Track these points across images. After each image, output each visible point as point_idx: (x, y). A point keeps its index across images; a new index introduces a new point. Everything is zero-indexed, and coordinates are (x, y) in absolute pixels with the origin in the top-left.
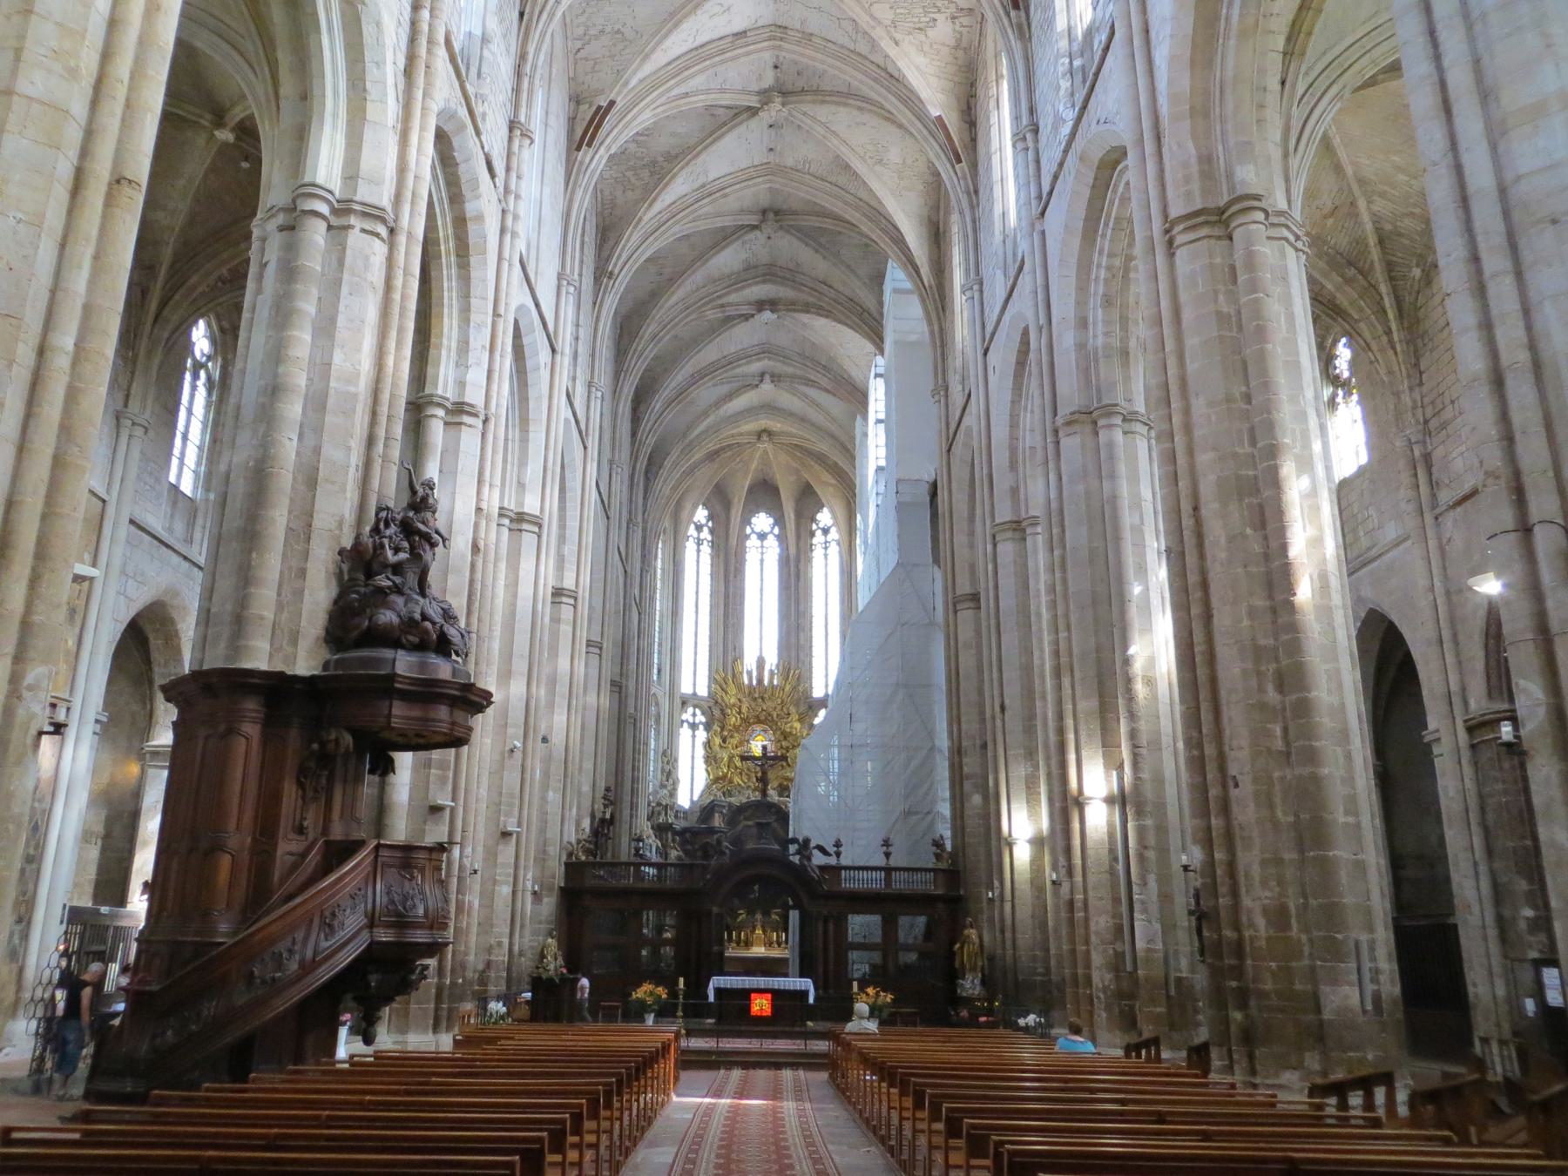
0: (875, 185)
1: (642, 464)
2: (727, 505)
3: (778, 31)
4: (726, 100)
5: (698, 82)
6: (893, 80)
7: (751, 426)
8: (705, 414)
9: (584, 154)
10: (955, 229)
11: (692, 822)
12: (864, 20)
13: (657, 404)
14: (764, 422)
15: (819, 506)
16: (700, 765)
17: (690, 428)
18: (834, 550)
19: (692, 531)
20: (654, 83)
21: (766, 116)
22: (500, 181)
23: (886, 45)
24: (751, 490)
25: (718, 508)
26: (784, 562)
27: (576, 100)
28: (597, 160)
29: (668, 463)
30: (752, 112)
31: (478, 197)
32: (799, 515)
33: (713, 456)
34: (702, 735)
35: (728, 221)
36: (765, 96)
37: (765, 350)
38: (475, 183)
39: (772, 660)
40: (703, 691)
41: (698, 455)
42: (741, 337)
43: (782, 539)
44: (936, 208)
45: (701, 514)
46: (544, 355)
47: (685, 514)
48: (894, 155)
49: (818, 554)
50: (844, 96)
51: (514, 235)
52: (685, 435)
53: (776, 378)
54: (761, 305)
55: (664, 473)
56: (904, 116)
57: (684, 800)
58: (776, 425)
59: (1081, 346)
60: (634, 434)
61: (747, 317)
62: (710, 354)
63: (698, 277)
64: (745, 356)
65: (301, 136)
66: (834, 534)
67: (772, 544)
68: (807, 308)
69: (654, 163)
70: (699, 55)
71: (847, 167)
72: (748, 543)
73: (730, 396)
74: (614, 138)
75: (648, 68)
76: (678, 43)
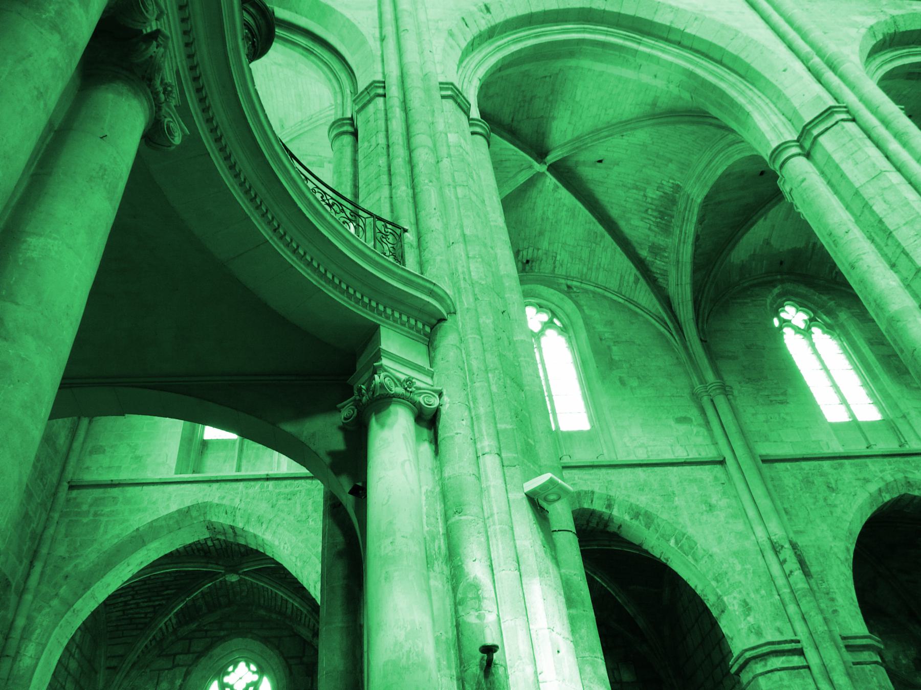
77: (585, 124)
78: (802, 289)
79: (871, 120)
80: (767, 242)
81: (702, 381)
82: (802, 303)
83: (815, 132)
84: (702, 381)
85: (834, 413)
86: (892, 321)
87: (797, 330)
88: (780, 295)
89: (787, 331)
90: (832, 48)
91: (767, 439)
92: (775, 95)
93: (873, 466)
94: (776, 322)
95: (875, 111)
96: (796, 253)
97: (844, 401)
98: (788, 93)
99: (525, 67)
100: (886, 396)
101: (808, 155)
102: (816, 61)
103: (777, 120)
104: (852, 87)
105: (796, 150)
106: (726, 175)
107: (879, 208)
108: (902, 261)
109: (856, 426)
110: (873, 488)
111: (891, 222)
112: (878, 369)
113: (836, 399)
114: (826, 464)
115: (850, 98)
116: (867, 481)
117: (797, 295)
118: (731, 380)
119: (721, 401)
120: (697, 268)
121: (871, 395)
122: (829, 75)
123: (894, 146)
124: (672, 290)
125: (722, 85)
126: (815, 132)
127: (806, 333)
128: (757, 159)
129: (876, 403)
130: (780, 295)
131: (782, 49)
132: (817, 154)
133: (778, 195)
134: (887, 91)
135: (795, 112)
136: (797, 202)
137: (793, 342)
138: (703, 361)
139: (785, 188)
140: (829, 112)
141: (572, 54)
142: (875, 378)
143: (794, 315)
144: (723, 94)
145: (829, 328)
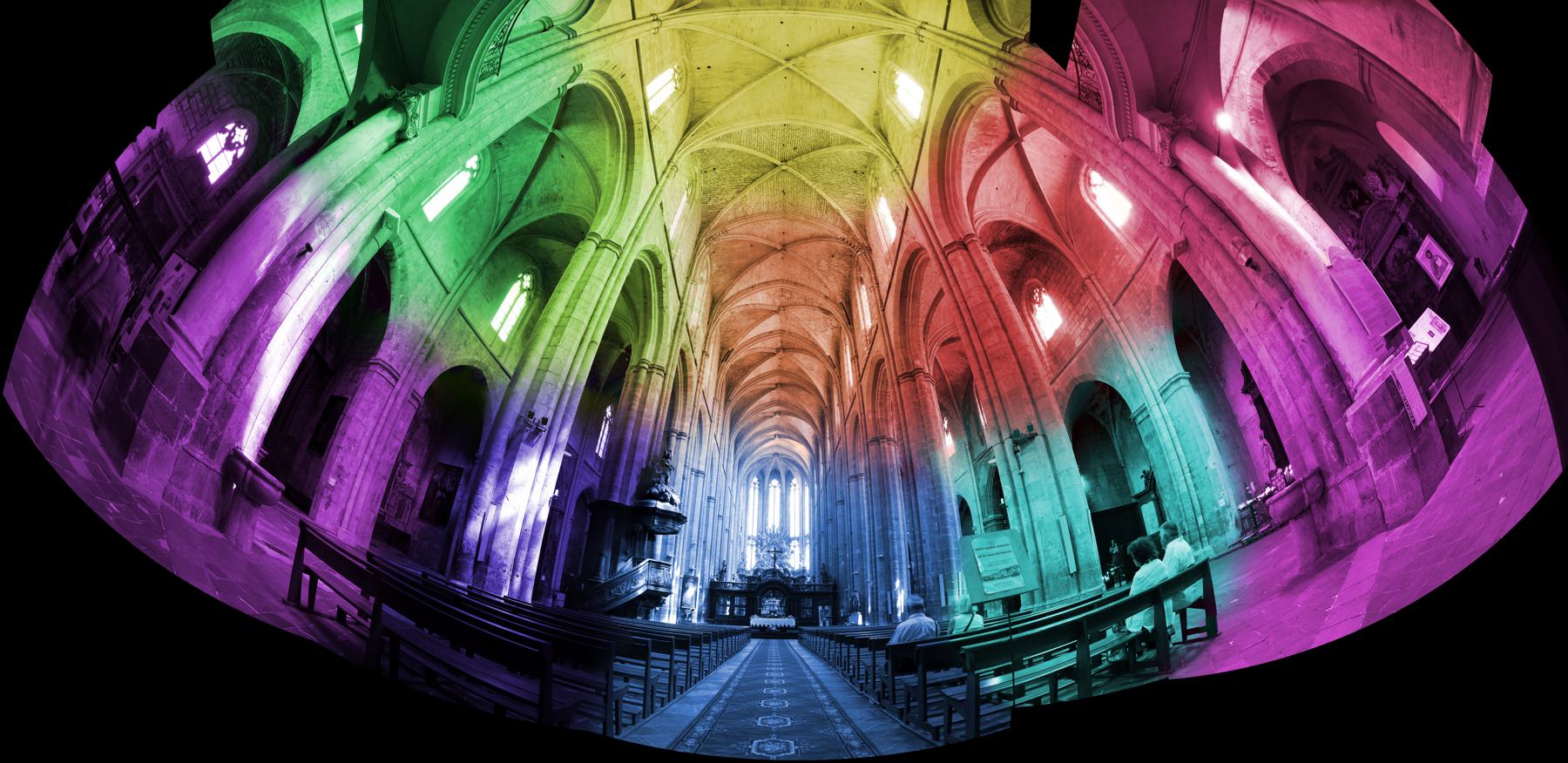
0: (810, 376)
1: (737, 462)
2: (764, 477)
3: (782, 332)
4: (767, 351)
5: (758, 345)
6: (816, 345)
8: (757, 447)
9: (724, 364)
10: (835, 389)
11: (751, 574)
12: (806, 328)
13: (743, 443)
14: (776, 450)
15: (793, 477)
16: (754, 558)
17: (753, 451)
20: (745, 345)
21: (778, 356)
23: (813, 335)
24: (772, 472)
26: (782, 495)
27: (722, 348)
28: (727, 366)
30: (774, 354)
33: (759, 461)
34: (755, 548)
35: (766, 387)
36: (778, 350)
37: (776, 428)
39: (777, 526)
40: (755, 535)
41: (755, 460)
42: (769, 423)
43: (781, 487)
44: (828, 383)
45: (755, 480)
48: (816, 368)
49: (792, 493)
50: (802, 350)
53: (780, 436)
54: (775, 413)
56: (819, 355)
57: (748, 568)
58: (779, 451)
61: (771, 417)
62: (759, 428)
63: (757, 404)
64: (770, 429)
66: (797, 486)
68: (789, 414)
69: (744, 368)
70: (759, 338)
71: (802, 371)
73: (766, 441)
74: (733, 360)
75: (744, 340)
76: (753, 333)
77: (579, 142)
78: (540, 278)
79: (620, 266)
80: (554, 251)
81: (478, 260)
82: (534, 282)
83: (608, 246)
84: (478, 260)
85: (495, 323)
86: (545, 320)
87: (521, 286)
88: (533, 270)
89: (519, 282)
90: (643, 235)
91: (469, 304)
92: (617, 223)
93: (484, 352)
94: (520, 276)
95: (624, 264)
96: (554, 266)
97: (502, 324)
98: (620, 226)
99: (599, 103)
100: (514, 338)
101: (597, 248)
102: (637, 231)
103: (608, 227)
104: (631, 251)
105: (598, 241)
106: (576, 217)
107: (587, 287)
108: (570, 309)
109: (496, 335)
110: (476, 358)
111: (584, 295)
112: (523, 328)
113: (501, 320)
114: (474, 335)
115: (626, 252)
116: (477, 354)
117: (537, 279)
118: (486, 272)
119: (474, 273)
120: (528, 227)
121: (511, 332)
122: (633, 239)
123: (614, 279)
124: (513, 221)
125: (615, 197)
126: (608, 246)
127: (522, 290)
128: (588, 227)
129: (509, 336)
130: (533, 270)
131: (638, 215)
132: (599, 252)
133: (575, 243)
134: (634, 264)
135: (614, 233)
136: (576, 254)
137: (516, 287)
138: (487, 256)
139: (580, 246)
140: (618, 247)
141: (610, 123)
142: (519, 328)
143: (527, 281)
144: (611, 199)
145: (529, 299)
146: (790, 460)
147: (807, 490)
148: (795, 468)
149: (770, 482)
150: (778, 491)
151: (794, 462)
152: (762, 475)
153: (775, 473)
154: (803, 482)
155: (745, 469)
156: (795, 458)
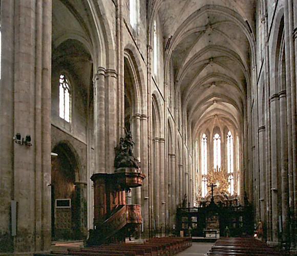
2: (209, 133)
7: (213, 114)
17: (200, 116)
18: (232, 140)
19: (202, 140)
22: (146, 61)
25: (208, 134)
29: (196, 125)
31: (140, 65)
32: (224, 133)
33: (205, 122)
38: (141, 63)
41: (203, 121)
45: (204, 136)
46: (162, 102)
47: (201, 136)
49: (228, 141)
51: (150, 73)
52: (199, 118)
55: (195, 127)
58: (218, 113)
59: (276, 76)
60: (188, 119)
65: (97, 56)
66: (231, 137)
67: (219, 140)
72: (214, 141)
146: (226, 118)
147: (238, 139)
148: (229, 124)
149: (213, 136)
150: (219, 141)
151: (228, 119)
152: (208, 132)
153: (217, 130)
154: (235, 133)
155: (196, 130)
156: (228, 116)
